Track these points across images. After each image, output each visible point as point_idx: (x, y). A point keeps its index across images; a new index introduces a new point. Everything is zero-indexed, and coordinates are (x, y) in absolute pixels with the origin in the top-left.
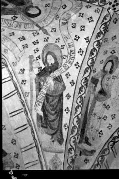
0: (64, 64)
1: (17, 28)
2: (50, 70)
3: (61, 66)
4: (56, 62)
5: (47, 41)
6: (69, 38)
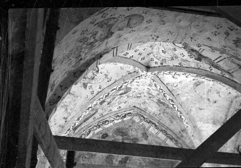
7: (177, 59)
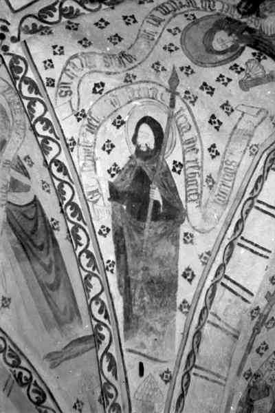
0: (206, 10)
1: (198, 146)
2: (246, 33)
3: (218, 14)
4: (218, 26)
5: (189, 68)
6: (145, 31)
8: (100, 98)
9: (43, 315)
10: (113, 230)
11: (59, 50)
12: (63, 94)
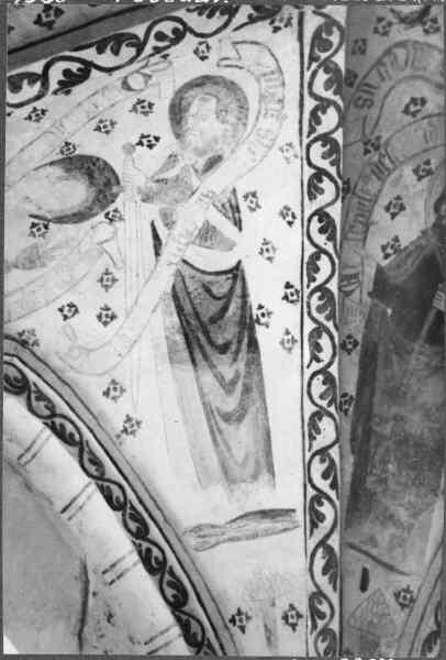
7: (373, 172)
8: (410, 124)
9: (199, 460)
10: (363, 346)
11: (384, 27)
12: (360, 102)
